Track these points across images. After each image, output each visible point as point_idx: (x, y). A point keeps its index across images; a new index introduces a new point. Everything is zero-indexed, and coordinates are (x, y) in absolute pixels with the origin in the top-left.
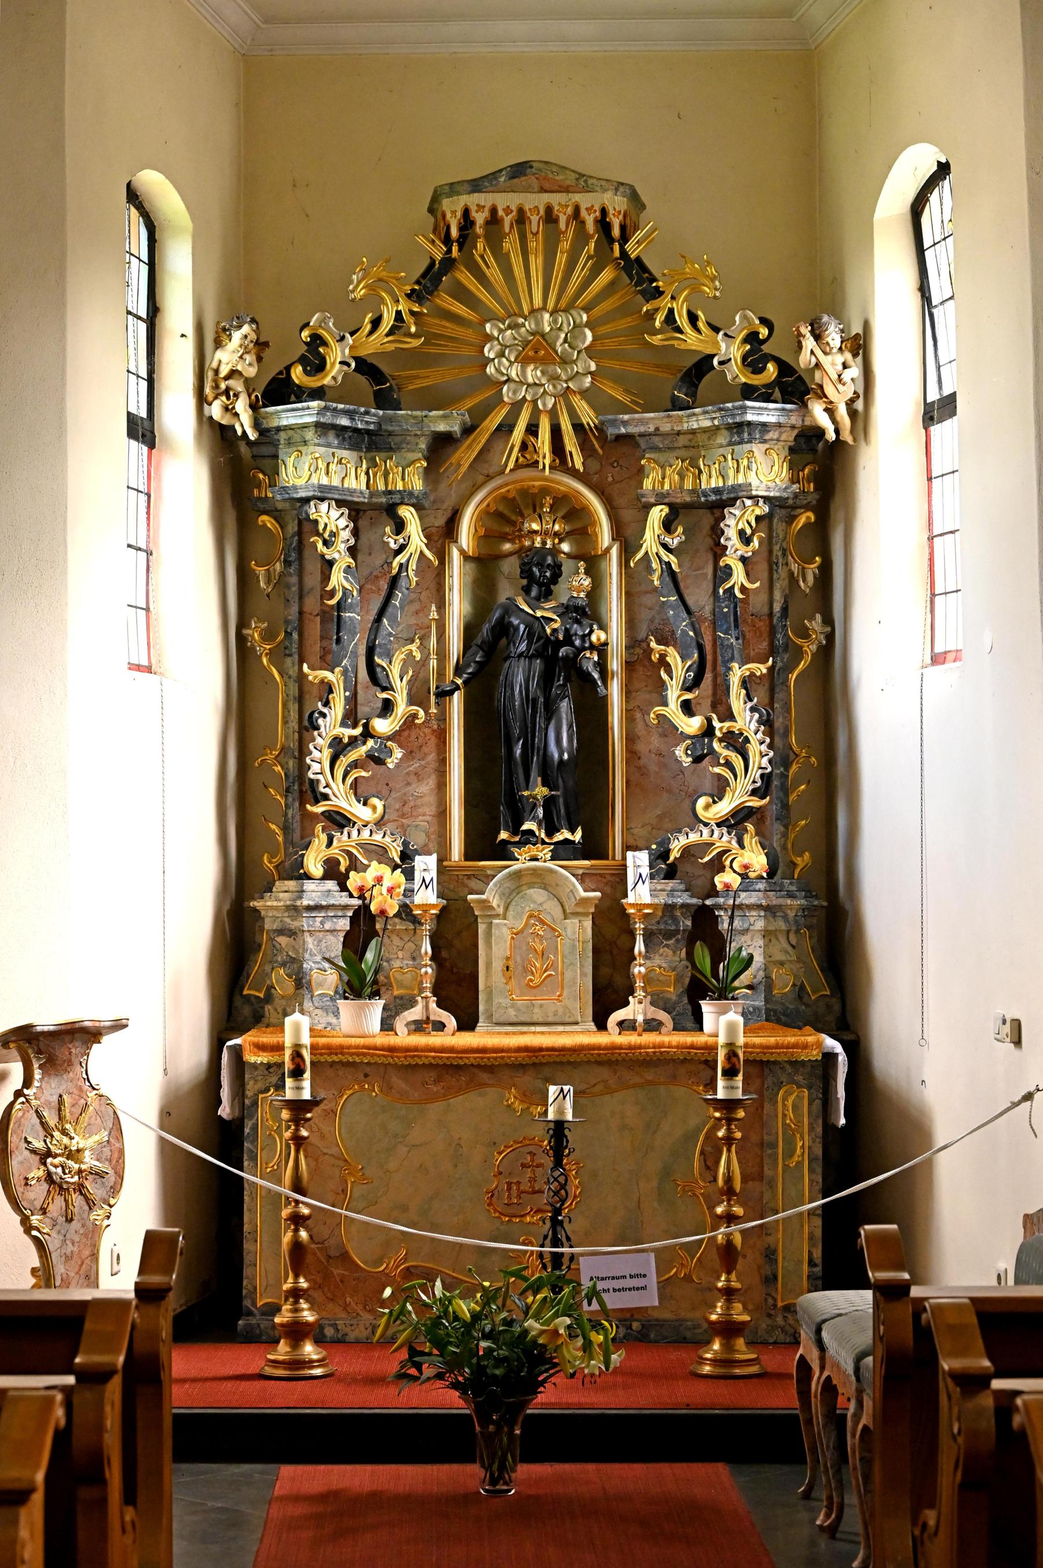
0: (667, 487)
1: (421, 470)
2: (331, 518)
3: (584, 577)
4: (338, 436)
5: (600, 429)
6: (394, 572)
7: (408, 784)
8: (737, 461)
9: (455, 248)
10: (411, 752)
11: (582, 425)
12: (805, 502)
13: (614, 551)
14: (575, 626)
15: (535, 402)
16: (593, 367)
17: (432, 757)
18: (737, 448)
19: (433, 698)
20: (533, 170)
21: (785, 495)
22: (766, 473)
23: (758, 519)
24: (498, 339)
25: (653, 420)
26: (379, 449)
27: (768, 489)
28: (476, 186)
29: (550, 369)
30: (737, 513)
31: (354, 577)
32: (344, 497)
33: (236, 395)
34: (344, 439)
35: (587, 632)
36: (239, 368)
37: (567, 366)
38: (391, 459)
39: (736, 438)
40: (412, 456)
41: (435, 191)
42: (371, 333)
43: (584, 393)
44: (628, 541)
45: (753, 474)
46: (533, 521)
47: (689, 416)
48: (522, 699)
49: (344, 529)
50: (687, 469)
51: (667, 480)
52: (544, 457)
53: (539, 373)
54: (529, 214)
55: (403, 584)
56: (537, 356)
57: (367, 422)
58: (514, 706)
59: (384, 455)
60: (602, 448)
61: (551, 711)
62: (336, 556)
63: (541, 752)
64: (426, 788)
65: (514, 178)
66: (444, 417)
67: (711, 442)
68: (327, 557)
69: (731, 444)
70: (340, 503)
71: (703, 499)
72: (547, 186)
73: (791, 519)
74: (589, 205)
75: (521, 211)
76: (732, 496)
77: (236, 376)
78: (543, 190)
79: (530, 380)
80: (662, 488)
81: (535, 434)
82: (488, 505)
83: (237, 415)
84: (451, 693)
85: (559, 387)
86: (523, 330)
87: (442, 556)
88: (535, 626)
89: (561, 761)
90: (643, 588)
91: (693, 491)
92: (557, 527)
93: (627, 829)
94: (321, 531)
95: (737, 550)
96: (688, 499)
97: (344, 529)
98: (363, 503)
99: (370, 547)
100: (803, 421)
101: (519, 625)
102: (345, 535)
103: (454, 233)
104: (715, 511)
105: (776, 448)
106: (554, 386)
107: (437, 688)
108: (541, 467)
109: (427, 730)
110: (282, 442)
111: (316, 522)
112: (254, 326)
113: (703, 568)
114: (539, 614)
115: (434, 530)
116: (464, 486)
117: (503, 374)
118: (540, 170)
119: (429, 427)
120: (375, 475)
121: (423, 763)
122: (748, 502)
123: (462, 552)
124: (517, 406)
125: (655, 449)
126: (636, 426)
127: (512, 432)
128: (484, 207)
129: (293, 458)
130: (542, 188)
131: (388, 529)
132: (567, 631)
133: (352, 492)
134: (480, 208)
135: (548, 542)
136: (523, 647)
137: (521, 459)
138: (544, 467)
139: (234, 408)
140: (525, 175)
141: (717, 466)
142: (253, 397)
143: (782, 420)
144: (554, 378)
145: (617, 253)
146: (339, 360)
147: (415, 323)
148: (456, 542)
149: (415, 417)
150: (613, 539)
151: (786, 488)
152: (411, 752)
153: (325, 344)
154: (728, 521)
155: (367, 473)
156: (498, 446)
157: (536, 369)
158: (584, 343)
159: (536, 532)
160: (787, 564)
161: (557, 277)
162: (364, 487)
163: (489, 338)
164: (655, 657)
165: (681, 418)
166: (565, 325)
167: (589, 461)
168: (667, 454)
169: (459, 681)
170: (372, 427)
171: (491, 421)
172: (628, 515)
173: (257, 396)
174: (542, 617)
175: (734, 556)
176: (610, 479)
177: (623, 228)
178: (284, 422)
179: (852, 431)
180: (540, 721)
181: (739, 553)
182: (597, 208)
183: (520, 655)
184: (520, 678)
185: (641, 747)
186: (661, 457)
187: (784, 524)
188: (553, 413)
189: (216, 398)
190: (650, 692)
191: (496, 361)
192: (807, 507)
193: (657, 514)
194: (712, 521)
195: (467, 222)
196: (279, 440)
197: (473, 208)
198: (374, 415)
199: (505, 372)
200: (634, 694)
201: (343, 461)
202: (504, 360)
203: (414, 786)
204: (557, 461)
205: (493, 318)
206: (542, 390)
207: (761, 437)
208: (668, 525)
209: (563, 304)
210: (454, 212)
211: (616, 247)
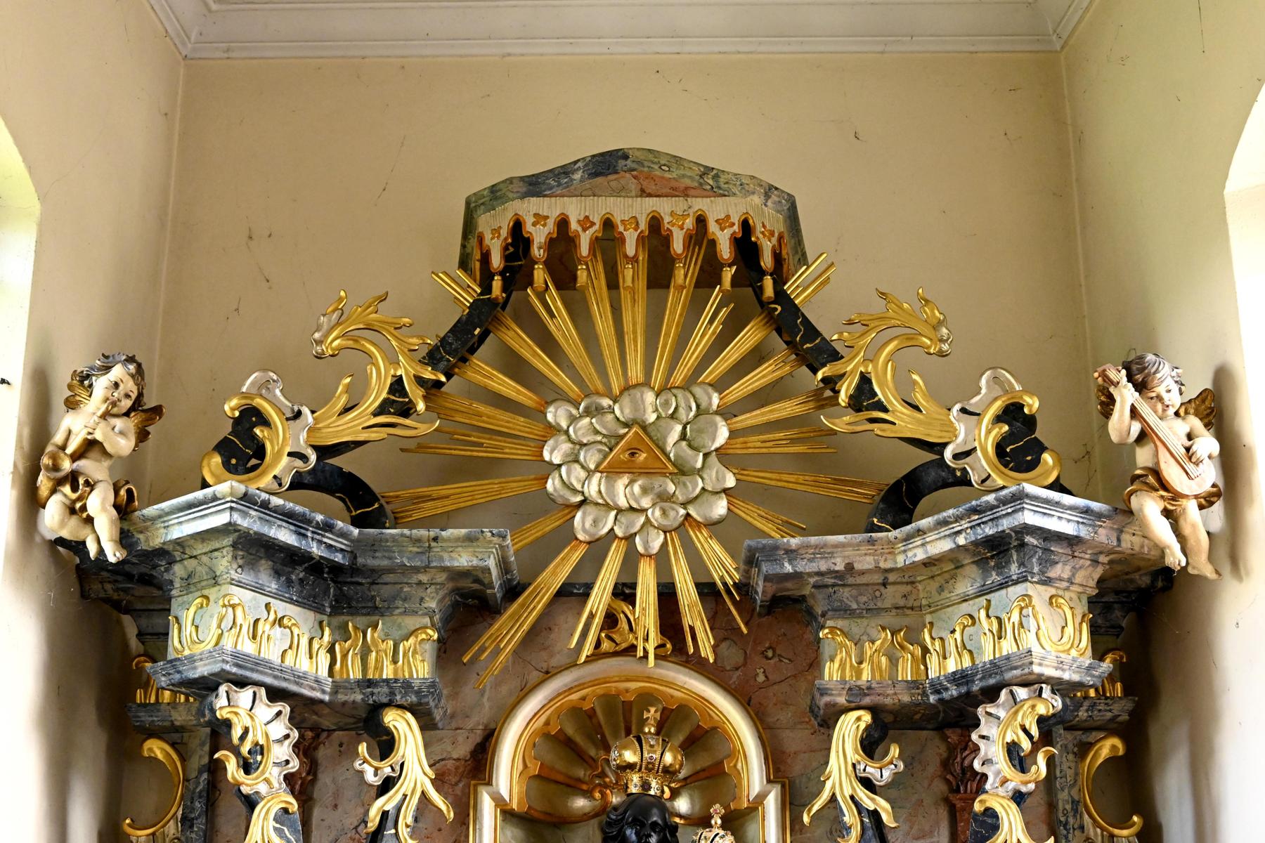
0: (866, 675)
1: (428, 646)
2: (258, 721)
3: (722, 833)
4: (277, 574)
5: (744, 587)
6: (373, 825)
8: (999, 619)
9: (497, 283)
11: (714, 584)
12: (1109, 715)
13: (772, 803)
15: (630, 538)
16: (730, 482)
18: (995, 597)
20: (629, 162)
21: (1088, 680)
22: (1056, 638)
23: (1041, 721)
24: (567, 432)
25: (845, 550)
26: (354, 612)
27: (1060, 665)
28: (535, 185)
29: (657, 482)
30: (1002, 714)
31: (294, 832)
32: (284, 685)
33: (90, 485)
34: (289, 583)
36: (98, 436)
37: (684, 478)
38: (375, 627)
39: (995, 577)
40: (411, 622)
41: (468, 203)
42: (347, 410)
43: (713, 526)
44: (794, 779)
45: (1032, 636)
46: (625, 747)
47: (908, 538)
49: (279, 741)
50: (902, 647)
51: (866, 667)
52: (646, 639)
53: (636, 488)
54: (621, 229)
56: (637, 469)
57: (329, 547)
59: (361, 620)
60: (746, 624)
62: (262, 788)
65: (596, 174)
66: (470, 539)
67: (946, 594)
68: (245, 790)
69: (984, 591)
70: (275, 694)
71: (932, 699)
72: (651, 188)
73: (1083, 749)
74: (723, 216)
75: (608, 224)
76: (992, 681)
77: (94, 453)
78: (643, 193)
79: (623, 503)
81: (631, 599)
82: (547, 723)
83: (90, 520)
85: (672, 514)
86: (610, 417)
91: (914, 685)
92: (668, 758)
94: (236, 741)
95: (1004, 781)
96: (906, 699)
97: (279, 741)
98: (321, 701)
99: (336, 795)
100: (1119, 540)
102: (283, 752)
103: (496, 261)
104: (948, 732)
105: (1067, 595)
106: (664, 512)
108: (640, 653)
110: (177, 585)
111: (228, 724)
112: (132, 367)
113: (931, 833)
115: (450, 764)
116: (504, 689)
117: (575, 491)
118: (640, 163)
119: (441, 559)
120: (345, 656)
122: (1022, 693)
123: (498, 800)
124: (598, 547)
125: (845, 612)
126: (811, 560)
127: (587, 595)
128: (547, 217)
129: (193, 609)
130: (643, 191)
131: (363, 748)
133: (300, 678)
134: (540, 219)
135: (654, 784)
137: (606, 646)
138: (646, 656)
139: (84, 508)
140: (616, 172)
141: (957, 635)
142: (123, 492)
143: (1084, 532)
144: (664, 498)
145: (769, 291)
146: (288, 449)
147: (425, 398)
148: (489, 783)
149: (418, 541)
150: (769, 781)
151: (1090, 668)
153: (265, 423)
154: (984, 729)
155: (331, 651)
156: (562, 619)
157: (632, 482)
158: (714, 440)
159: (631, 767)
160: (1082, 828)
161: (667, 335)
162: (323, 672)
163: (553, 430)
165: (891, 543)
166: (682, 411)
167: (724, 645)
168: (865, 622)
170: (338, 558)
171: (554, 573)
172: (795, 739)
173: (129, 492)
175: (1001, 791)
176: (761, 678)
177: (778, 258)
178: (177, 533)
179: (1211, 558)
181: (1011, 786)
182: (736, 219)
186: (856, 627)
187: (1071, 757)
188: (662, 560)
189: (53, 491)
191: (564, 469)
192: (1110, 728)
193: (851, 727)
194: (943, 750)
195: (518, 239)
196: (171, 582)
197: (529, 221)
198: (343, 534)
199: (579, 487)
201: (285, 621)
202: (577, 466)
204: (669, 646)
205: (560, 396)
206: (642, 519)
207: (1042, 572)
208: (871, 745)
209: (679, 376)
210: (496, 231)
211: (768, 282)
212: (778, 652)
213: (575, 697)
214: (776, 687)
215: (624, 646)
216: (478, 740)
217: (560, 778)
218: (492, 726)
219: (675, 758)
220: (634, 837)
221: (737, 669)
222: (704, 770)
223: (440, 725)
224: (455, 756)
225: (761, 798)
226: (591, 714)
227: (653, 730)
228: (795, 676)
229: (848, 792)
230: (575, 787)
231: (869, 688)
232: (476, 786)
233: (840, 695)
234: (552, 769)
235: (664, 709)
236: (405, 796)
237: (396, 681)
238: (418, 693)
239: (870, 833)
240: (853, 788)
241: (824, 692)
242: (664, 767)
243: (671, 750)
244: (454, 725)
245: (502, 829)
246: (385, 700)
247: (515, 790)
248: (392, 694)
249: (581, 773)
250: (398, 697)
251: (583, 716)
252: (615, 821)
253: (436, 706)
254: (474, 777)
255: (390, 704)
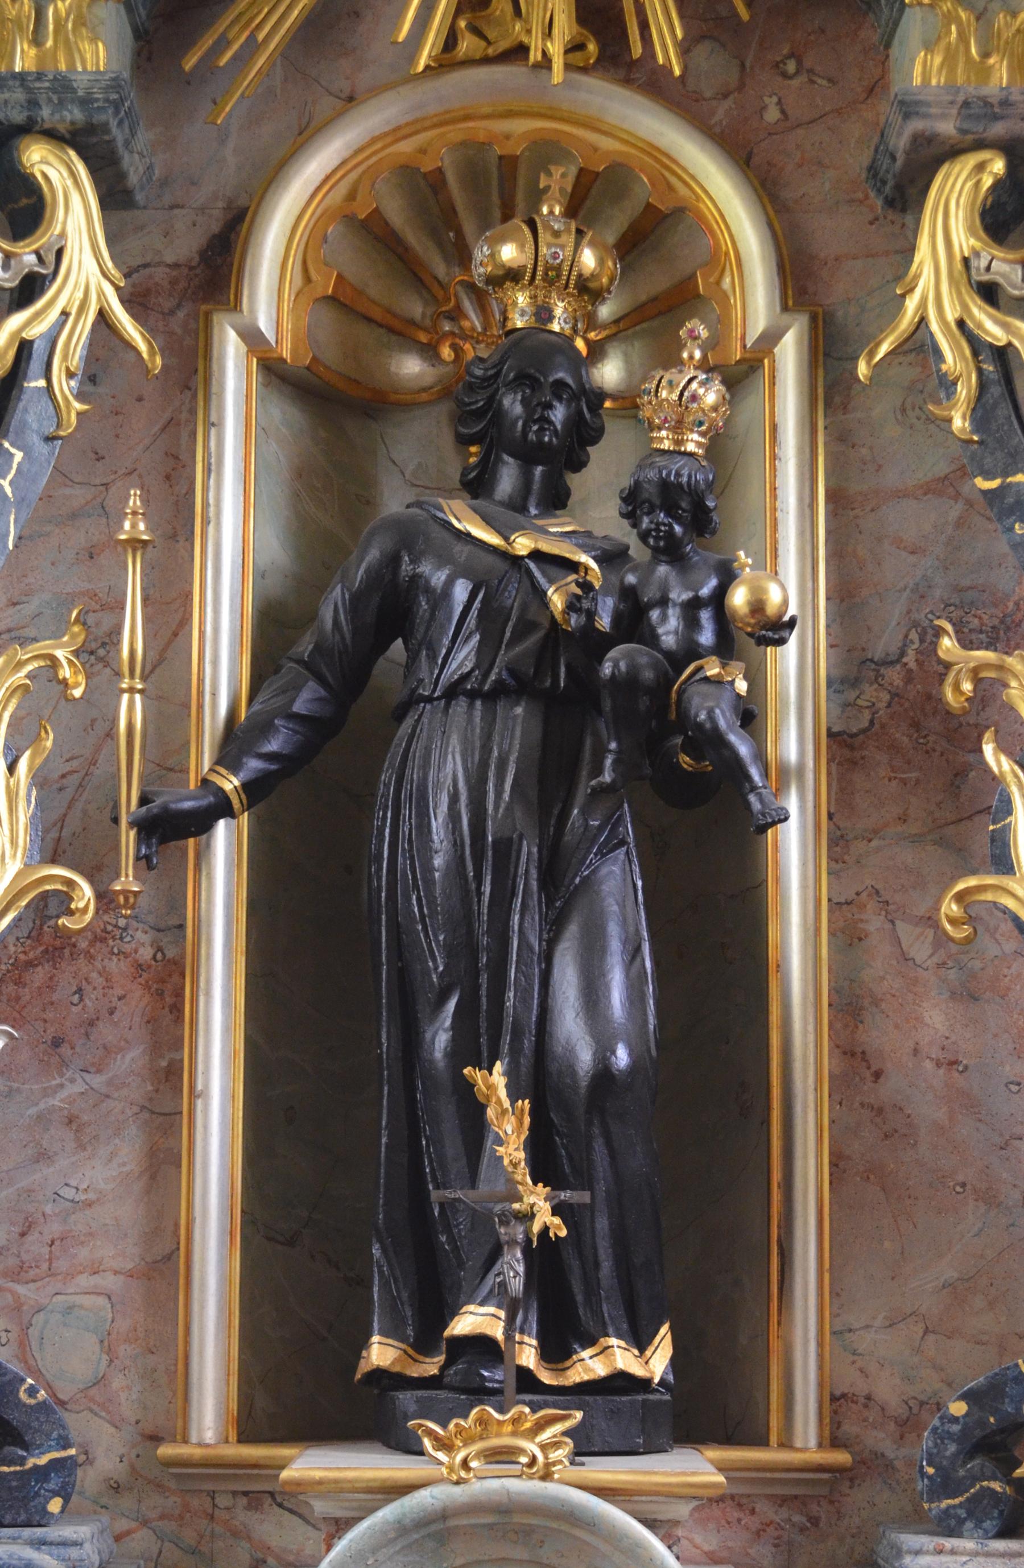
7: (43, 1157)
10: (57, 1043)
13: (789, 354)
14: (663, 569)
17: (132, 1059)
19: (128, 838)
35: (705, 592)
48: (457, 845)
52: (548, 33)
55: (31, 419)
58: (428, 868)
61: (562, 891)
63: (528, 1043)
64: (102, 1173)
80: (984, 72)
84: (199, 823)
87: (190, 371)
88: (505, 578)
89: (604, 1073)
90: (891, 478)
93: (836, 1335)
101: (450, 583)
107: (144, 801)
108: (535, 55)
109: (114, 965)
114: (522, 545)
115: (160, 274)
121: (97, 1081)
123: (252, 337)
132: (629, 595)
135: (559, 309)
136: (464, 658)
137: (467, 45)
148: (237, 307)
150: (785, 308)
152: (57, 1043)
164: (957, 693)
167: (702, 51)
169: (230, 783)
172: (833, 232)
174: (536, 555)
176: (772, 115)
180: (524, 925)
183: (452, 692)
184: (451, 768)
185: (880, 1035)
190: (916, 839)
200: (859, 847)
203: (63, 1162)
204: (592, 47)
212: (808, 63)
213: (406, 147)
214: (800, 131)
215: (503, 45)
216: (216, 228)
217: (377, 314)
218: (242, 202)
219: (601, 262)
220: (518, 409)
221: (726, 96)
222: (654, 300)
223: (139, 197)
224: (170, 259)
225: (771, 338)
226: (436, 181)
227: (557, 210)
228: (838, 112)
229: (951, 315)
230: (401, 333)
231: (1005, 103)
232: (208, 316)
233: (944, 116)
234: (360, 293)
235: (581, 171)
236: (65, 314)
237: (40, 76)
238: (85, 102)
239: (996, 391)
240: (965, 307)
241: (909, 108)
242: (580, 275)
243: (592, 244)
244: (167, 199)
245: (261, 399)
246: (18, 117)
247: (287, 325)
248: (33, 103)
249: (416, 308)
250: (45, 112)
251: (426, 188)
252: (484, 379)
253: (127, 143)
254: (205, 300)
255: (28, 129)
